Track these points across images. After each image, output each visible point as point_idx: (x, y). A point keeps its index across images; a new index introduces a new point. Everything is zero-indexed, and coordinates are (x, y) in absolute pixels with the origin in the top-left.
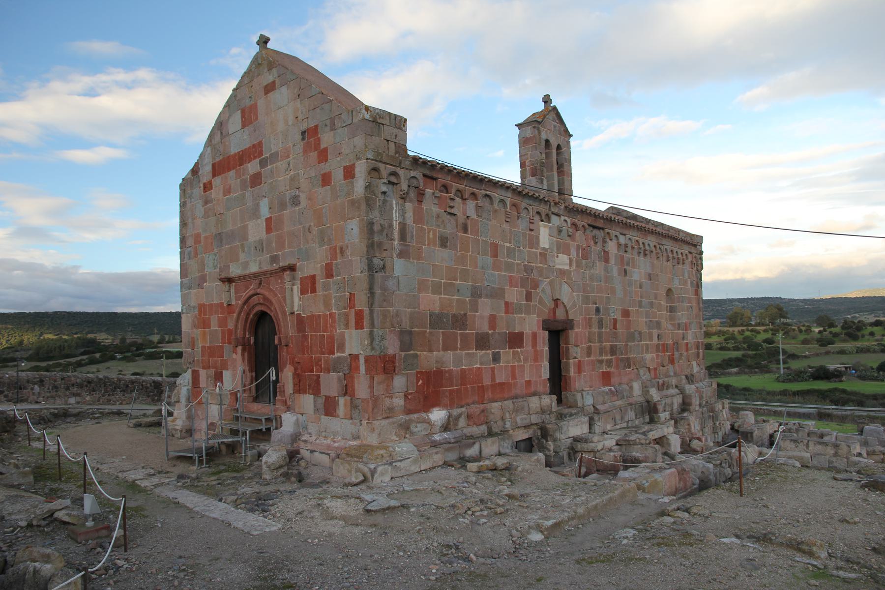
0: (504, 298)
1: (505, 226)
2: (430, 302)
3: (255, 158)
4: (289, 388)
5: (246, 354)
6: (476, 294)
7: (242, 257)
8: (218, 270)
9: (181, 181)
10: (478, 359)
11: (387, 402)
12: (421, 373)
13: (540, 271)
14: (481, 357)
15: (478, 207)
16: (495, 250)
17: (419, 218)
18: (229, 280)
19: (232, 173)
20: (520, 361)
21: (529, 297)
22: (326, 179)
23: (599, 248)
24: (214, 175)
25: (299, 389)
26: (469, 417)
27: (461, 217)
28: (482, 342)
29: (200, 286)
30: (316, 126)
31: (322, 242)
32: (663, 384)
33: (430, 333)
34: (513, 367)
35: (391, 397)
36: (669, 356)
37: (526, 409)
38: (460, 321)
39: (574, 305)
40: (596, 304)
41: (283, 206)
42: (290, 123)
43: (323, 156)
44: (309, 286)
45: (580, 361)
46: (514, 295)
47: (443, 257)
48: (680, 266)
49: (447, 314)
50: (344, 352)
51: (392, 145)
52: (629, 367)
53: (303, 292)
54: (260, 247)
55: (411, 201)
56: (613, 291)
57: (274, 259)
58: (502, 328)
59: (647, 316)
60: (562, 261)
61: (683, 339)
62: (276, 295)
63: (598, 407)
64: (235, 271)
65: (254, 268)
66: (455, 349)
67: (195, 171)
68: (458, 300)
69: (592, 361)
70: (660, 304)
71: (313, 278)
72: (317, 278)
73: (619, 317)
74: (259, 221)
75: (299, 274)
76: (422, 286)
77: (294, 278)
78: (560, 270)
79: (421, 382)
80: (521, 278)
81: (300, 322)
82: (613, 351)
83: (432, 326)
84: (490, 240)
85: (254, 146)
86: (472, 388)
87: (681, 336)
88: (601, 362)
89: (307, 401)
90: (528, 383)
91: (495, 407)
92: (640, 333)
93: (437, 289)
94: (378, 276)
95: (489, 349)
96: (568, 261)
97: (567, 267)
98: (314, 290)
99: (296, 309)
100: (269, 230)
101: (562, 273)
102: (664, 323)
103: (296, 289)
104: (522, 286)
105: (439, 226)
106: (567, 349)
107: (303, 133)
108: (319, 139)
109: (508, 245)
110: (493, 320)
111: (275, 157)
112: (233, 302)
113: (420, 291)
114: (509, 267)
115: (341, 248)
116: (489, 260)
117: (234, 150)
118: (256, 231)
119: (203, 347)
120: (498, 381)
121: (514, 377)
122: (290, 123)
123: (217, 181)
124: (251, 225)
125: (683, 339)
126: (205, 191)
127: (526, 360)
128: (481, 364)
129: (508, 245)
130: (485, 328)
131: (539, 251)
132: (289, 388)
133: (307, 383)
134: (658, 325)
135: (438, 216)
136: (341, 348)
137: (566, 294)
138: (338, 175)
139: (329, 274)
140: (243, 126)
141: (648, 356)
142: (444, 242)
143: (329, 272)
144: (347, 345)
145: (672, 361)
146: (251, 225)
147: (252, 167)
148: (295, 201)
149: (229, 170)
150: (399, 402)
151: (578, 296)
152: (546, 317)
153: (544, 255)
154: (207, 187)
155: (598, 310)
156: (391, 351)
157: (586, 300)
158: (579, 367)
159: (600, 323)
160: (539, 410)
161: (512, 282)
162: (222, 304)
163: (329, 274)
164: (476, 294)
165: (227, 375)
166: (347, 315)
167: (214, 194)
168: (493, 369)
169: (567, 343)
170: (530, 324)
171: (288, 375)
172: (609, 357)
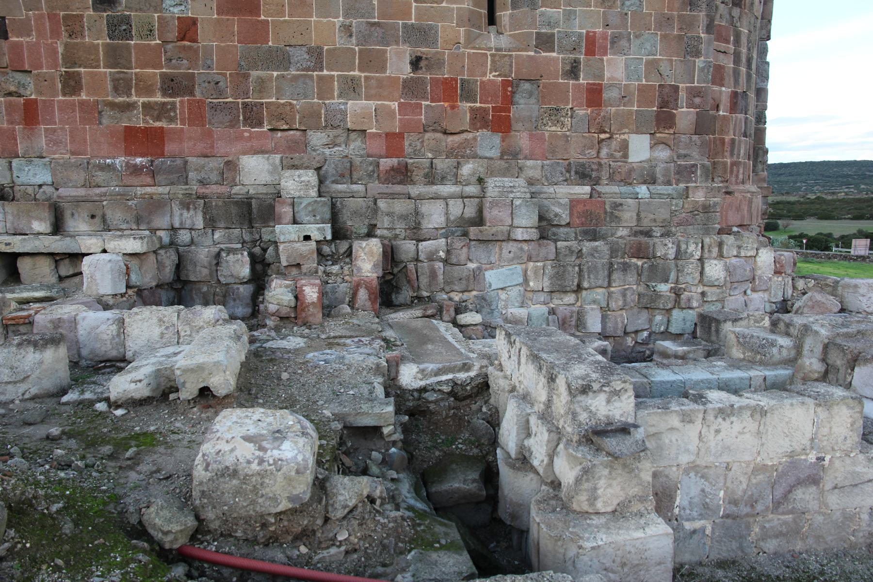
52: (260, 124)
69: (82, 103)
88: (129, 107)
125: (573, 71)
134: (421, 34)
141: (356, 108)
145: (501, 123)
172: (159, 98)
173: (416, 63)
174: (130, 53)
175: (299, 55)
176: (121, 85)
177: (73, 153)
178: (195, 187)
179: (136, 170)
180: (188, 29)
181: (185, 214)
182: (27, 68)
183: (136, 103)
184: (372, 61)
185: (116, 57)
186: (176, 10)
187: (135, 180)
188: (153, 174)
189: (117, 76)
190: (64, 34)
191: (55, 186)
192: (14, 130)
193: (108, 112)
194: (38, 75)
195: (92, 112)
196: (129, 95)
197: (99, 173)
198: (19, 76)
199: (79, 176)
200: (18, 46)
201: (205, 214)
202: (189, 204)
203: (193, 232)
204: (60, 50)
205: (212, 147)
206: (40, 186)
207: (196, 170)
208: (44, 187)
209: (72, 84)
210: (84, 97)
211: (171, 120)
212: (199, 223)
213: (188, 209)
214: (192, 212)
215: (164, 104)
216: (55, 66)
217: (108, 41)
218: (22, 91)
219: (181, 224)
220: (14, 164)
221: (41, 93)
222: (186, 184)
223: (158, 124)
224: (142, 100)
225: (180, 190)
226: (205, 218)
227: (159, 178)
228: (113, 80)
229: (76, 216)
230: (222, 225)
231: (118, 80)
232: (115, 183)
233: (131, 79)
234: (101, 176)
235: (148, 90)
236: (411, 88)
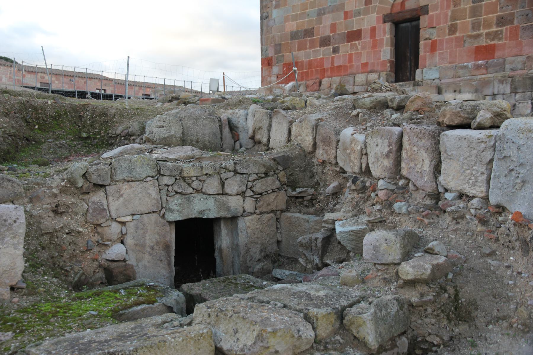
0: (344, 9)
2: (291, 26)
6: (321, 13)
10: (322, 53)
11: (269, 79)
12: (285, 64)
14: (324, 51)
20: (357, 49)
26: (307, 87)
28: (325, 42)
34: (351, 55)
35: (270, 77)
37: (352, 82)
38: (309, 32)
49: (301, 31)
58: (342, 30)
66: (306, 49)
68: (307, 21)
69: (456, 38)
76: (287, 19)
79: (285, 69)
86: (316, 70)
88: (479, 36)
90: (365, 65)
93: (295, 18)
94: (265, 21)
95: (330, 45)
110: (333, 27)
113: (285, 22)
120: (336, 65)
121: (350, 60)
127: (363, 48)
128: (323, 55)
130: (327, 33)
152: (386, 13)
156: (270, 55)
158: (433, 47)
160: (365, 83)
164: (321, 13)
168: (333, 58)
170: (370, 20)
172: (494, 29)
174: (482, 9)
176: (476, 26)
177: (450, 63)
178: (508, 73)
179: (478, 67)
181: (501, 86)
182: (434, 26)
183: (482, 33)
187: (477, 72)
188: (487, 68)
189: (474, 21)
190: (452, 6)
191: (440, 79)
192: (426, 55)
193: (468, 40)
194: (438, 28)
195: (460, 41)
196: (479, 30)
197: (461, 71)
198: (431, 30)
199: (451, 73)
201: (511, 85)
202: (503, 81)
203: (504, 96)
205: (521, 50)
206: (434, 80)
207: (510, 63)
208: (435, 80)
209: (453, 29)
210: (458, 34)
211: (500, 39)
212: (508, 90)
213: (503, 83)
214: (504, 85)
215: (497, 31)
216: (446, 22)
217: (472, 5)
218: (431, 37)
219: (498, 92)
220: (424, 71)
221: (439, 36)
222: (504, 71)
223: (493, 42)
224: (486, 31)
225: (500, 75)
226: (511, 88)
227: (489, 70)
229: (447, 91)
230: (521, 91)
231: (474, 23)
232: (467, 75)
233: (481, 22)
234: (461, 72)
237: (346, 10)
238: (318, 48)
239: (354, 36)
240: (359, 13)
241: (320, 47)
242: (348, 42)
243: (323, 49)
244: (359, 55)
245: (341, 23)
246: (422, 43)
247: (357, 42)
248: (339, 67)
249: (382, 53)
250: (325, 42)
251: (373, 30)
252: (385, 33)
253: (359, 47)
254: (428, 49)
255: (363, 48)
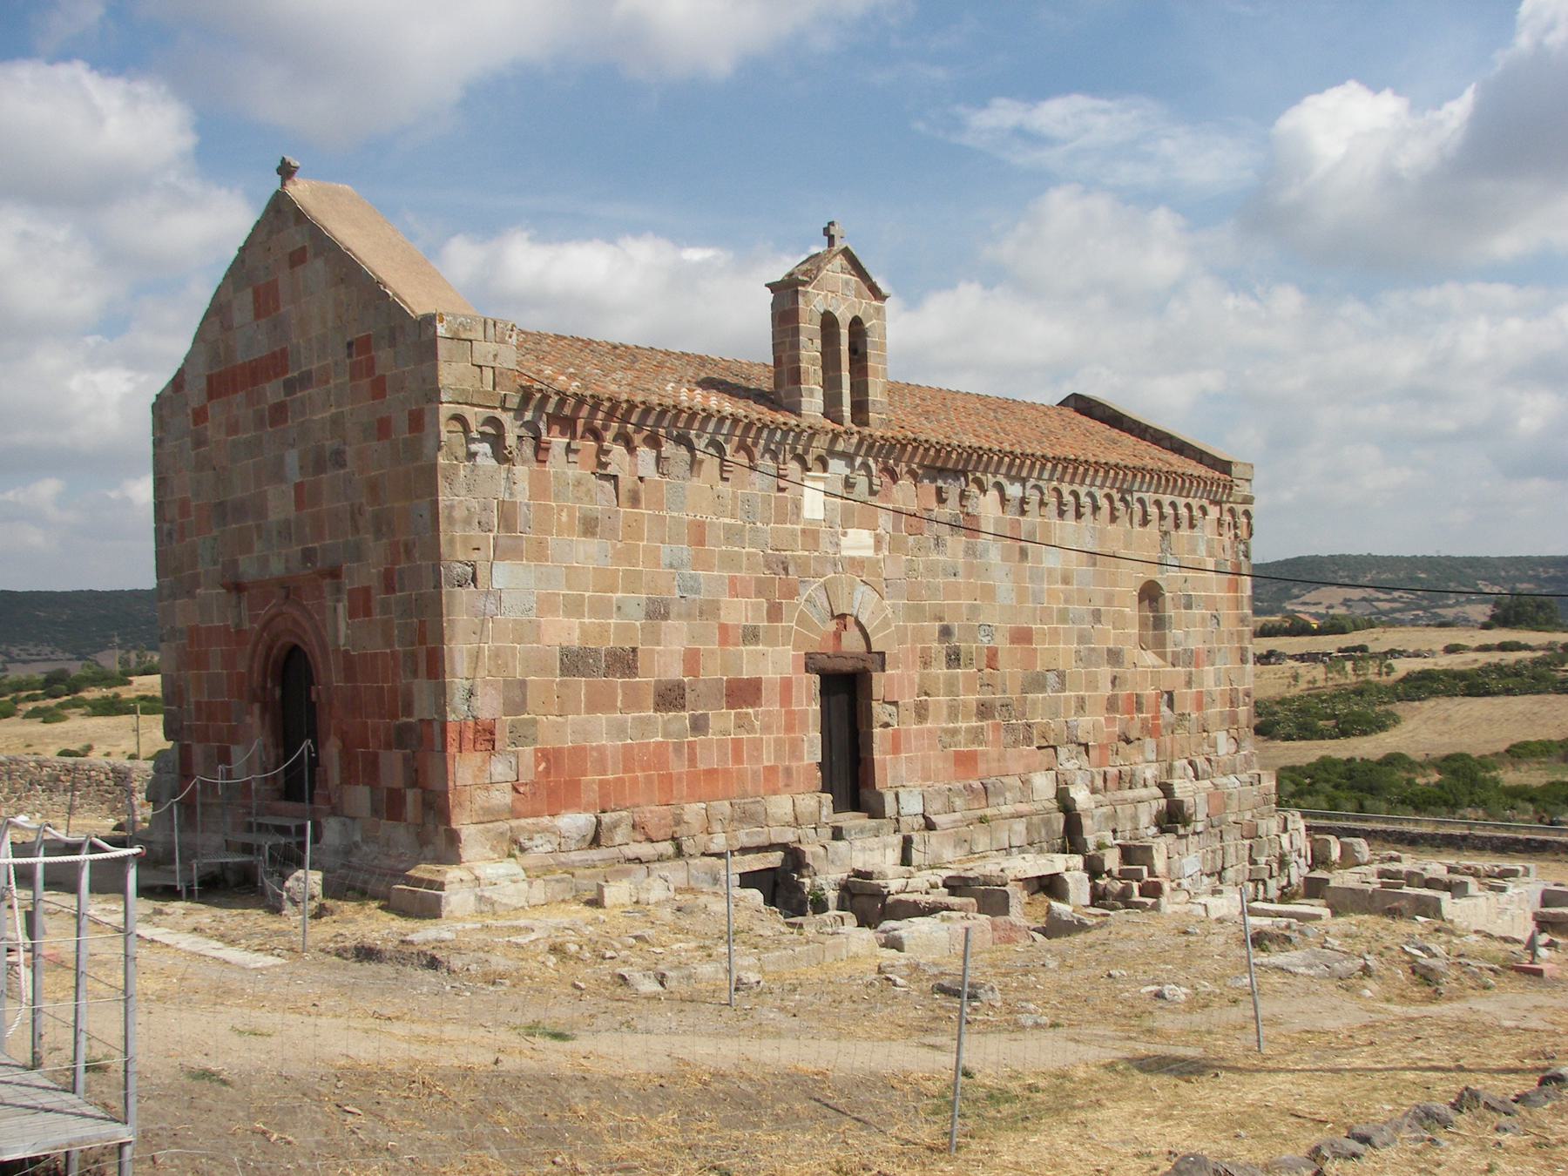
1: (722, 487)
2: (564, 631)
3: (277, 375)
4: (334, 775)
5: (267, 717)
6: (657, 612)
7: (258, 546)
8: (219, 567)
9: (154, 399)
13: (803, 565)
15: (659, 459)
16: (698, 534)
17: (540, 488)
18: (237, 587)
19: (240, 397)
20: (752, 730)
21: (775, 613)
22: (383, 428)
23: (951, 509)
24: (211, 397)
25: (349, 778)
27: (626, 482)
28: (670, 697)
29: (190, 594)
30: (369, 337)
31: (378, 533)
32: (1120, 776)
33: (561, 684)
36: (1144, 720)
38: (625, 662)
39: (886, 623)
40: (941, 619)
41: (319, 465)
42: (330, 324)
43: (379, 389)
44: (361, 604)
45: (897, 732)
46: (740, 611)
47: (589, 552)
48: (1184, 531)
49: (596, 651)
50: (410, 714)
51: (488, 374)
53: (352, 614)
54: (286, 531)
55: (524, 462)
56: (989, 592)
57: (308, 555)
58: (714, 672)
59: (1083, 638)
60: (858, 543)
61: (1189, 684)
62: (312, 618)
63: (934, 818)
64: (248, 568)
65: (277, 568)
66: (613, 708)
67: (178, 383)
68: (617, 625)
69: (929, 731)
70: (1122, 615)
71: (367, 591)
72: (373, 592)
73: (1002, 643)
74: (284, 487)
75: (347, 584)
76: (546, 604)
77: (338, 590)
78: (852, 559)
80: (758, 580)
81: (350, 665)
82: (984, 710)
83: (565, 670)
84: (687, 516)
85: (274, 355)
86: (649, 779)
87: (1183, 678)
88: (955, 732)
89: (360, 797)
91: (693, 811)
92: (1061, 676)
93: (574, 607)
95: (684, 707)
96: (871, 542)
97: (870, 553)
98: (368, 612)
99: (342, 641)
100: (300, 503)
101: (856, 564)
102: (1132, 651)
103: (342, 608)
104: (759, 593)
105: (579, 499)
106: (870, 708)
107: (350, 345)
108: (372, 358)
109: (727, 520)
110: (692, 660)
111: (305, 380)
112: (246, 626)
113: (541, 612)
114: (730, 561)
115: (406, 545)
116: (685, 551)
117: (241, 358)
118: (280, 505)
119: (198, 704)
120: (701, 766)
122: (330, 324)
123: (216, 410)
124: (271, 491)
125: (1189, 684)
126: (196, 423)
129: (727, 520)
130: (676, 672)
131: (799, 527)
132: (334, 775)
133: (362, 768)
134: (1114, 657)
135: (579, 483)
136: (408, 710)
137: (863, 603)
138: (401, 422)
139: (389, 588)
140: (258, 316)
142: (589, 527)
143: (389, 582)
144: (416, 705)
146: (271, 491)
147: (272, 392)
148: (339, 459)
149: (235, 391)
150: (502, 797)
151: (893, 606)
153: (811, 535)
154: (200, 416)
155: (946, 632)
156: (485, 715)
157: (916, 612)
159: (954, 658)
161: (735, 588)
162: (227, 627)
163: (389, 588)
164: (657, 612)
165: (236, 750)
166: (413, 656)
167: (212, 431)
169: (870, 697)
170: (778, 663)
171: (332, 750)
173: (1114, 681)
175: (1051, 677)
176: (953, 714)
180: (992, 657)
184: (1092, 684)
185: (951, 687)
186: (985, 640)
200: (891, 677)
204: (917, 680)
209: (921, 712)
223: (974, 748)
224: (964, 725)
228: (950, 707)
235: (967, 717)
236: (1112, 705)
237: (723, 620)
238: (651, 713)
239: (743, 693)
240: (751, 635)
241: (656, 710)
242: (731, 706)
243: (661, 717)
244: (757, 745)
245: (713, 652)
246: (877, 731)
247: (750, 711)
248: (710, 773)
249: (806, 745)
250: (670, 697)
251: (786, 685)
252: (810, 700)
253: (757, 724)
254: (888, 746)
255: (766, 728)
